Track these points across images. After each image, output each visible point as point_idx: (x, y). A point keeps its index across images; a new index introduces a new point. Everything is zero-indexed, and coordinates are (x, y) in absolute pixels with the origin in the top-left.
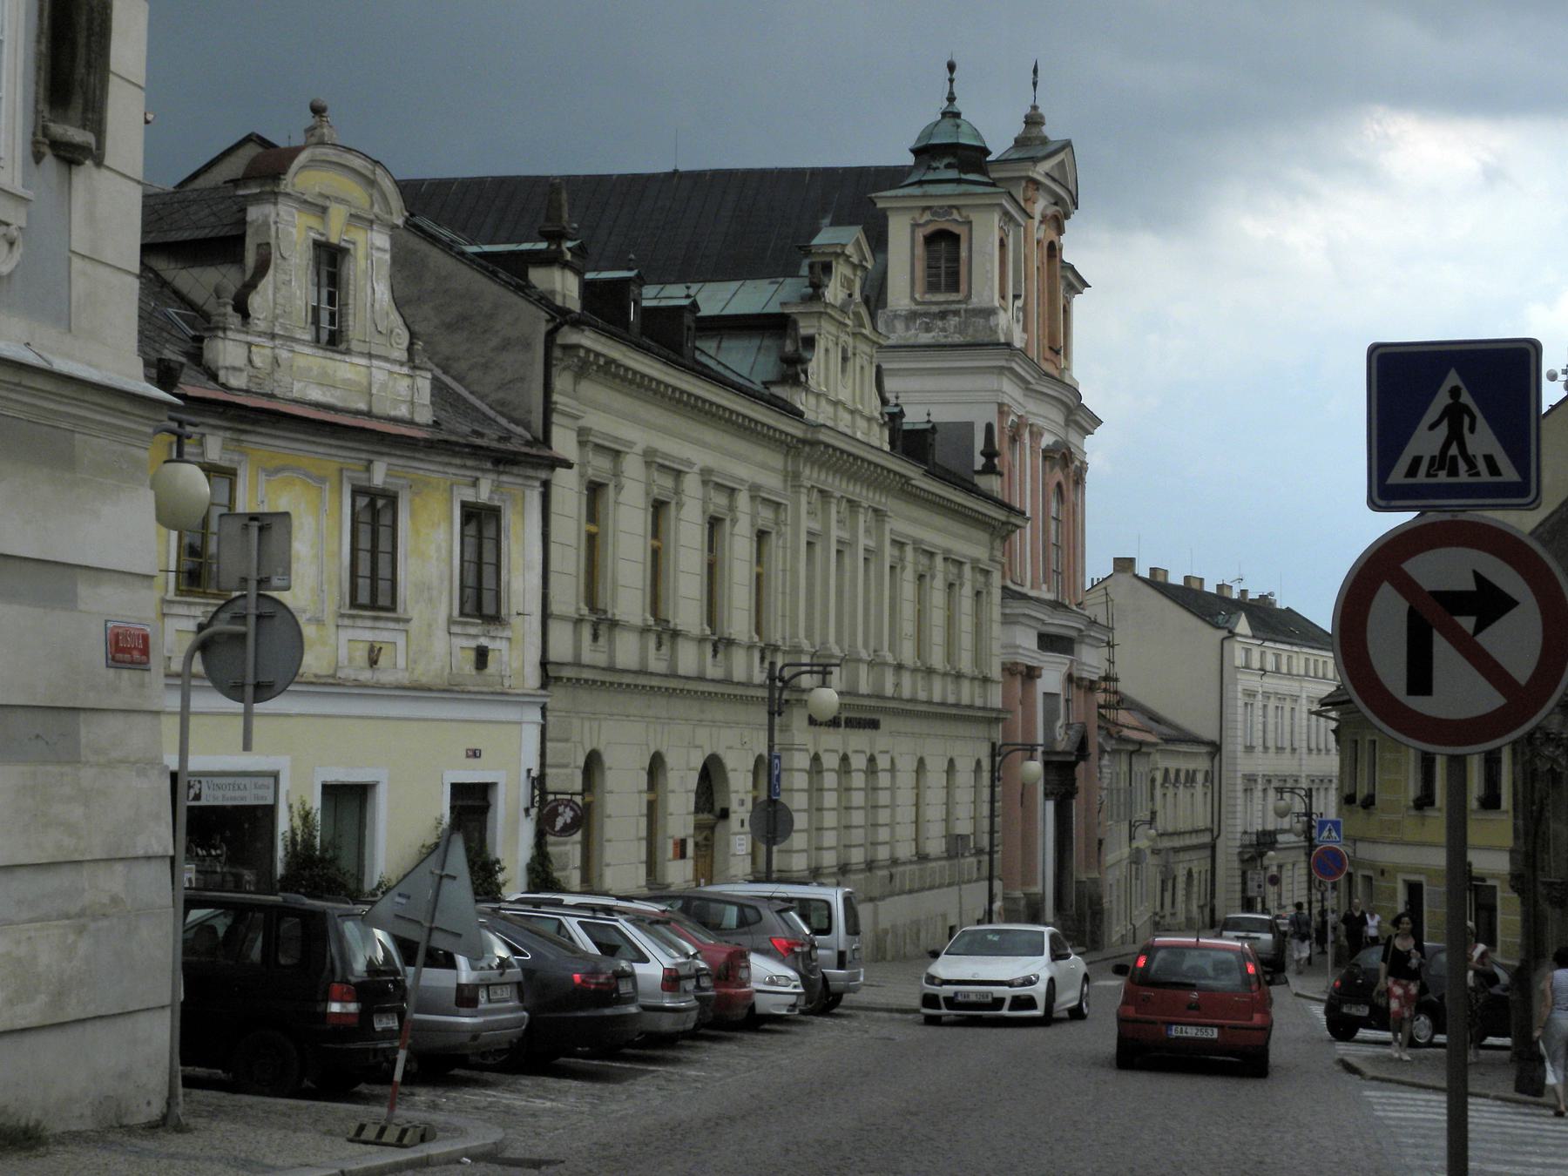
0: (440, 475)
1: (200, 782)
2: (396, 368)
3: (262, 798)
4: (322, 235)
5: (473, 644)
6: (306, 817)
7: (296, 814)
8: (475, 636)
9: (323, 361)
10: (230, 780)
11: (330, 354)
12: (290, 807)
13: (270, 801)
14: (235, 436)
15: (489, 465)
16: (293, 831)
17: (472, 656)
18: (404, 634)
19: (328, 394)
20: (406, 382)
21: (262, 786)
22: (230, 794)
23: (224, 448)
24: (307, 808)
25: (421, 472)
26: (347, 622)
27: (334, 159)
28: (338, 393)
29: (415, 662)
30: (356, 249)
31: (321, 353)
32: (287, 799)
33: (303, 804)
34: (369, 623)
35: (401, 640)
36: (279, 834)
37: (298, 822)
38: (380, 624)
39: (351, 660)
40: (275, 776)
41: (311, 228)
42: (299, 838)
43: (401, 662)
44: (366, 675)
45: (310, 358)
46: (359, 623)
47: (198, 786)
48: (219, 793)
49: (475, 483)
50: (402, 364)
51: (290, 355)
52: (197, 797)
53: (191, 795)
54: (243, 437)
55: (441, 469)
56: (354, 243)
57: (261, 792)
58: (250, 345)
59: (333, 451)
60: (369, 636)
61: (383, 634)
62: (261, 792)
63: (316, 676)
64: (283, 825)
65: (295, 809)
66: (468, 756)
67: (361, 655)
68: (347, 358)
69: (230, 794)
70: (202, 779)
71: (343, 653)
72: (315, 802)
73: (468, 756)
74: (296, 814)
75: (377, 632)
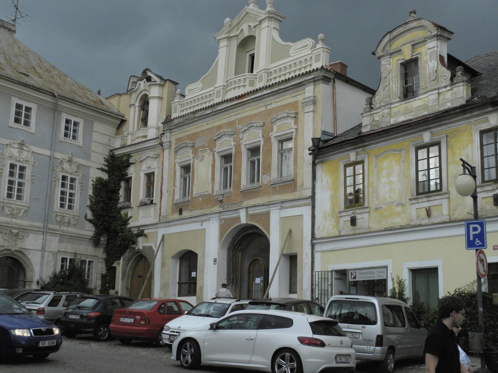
0: (465, 125)
1: (356, 272)
2: (444, 90)
3: (381, 277)
4: (403, 59)
5: (491, 194)
6: (401, 283)
7: (395, 282)
8: (493, 190)
9: (405, 105)
10: (368, 271)
11: (407, 101)
12: (393, 279)
13: (385, 278)
14: (363, 149)
15: (490, 109)
16: (394, 289)
17: (492, 200)
18: (446, 200)
19: (408, 116)
20: (449, 93)
21: (381, 272)
22: (367, 276)
23: (357, 154)
24: (400, 279)
25: (453, 128)
26: (414, 202)
27: (403, 30)
28: (413, 114)
29: (455, 210)
30: (421, 55)
31: (404, 102)
32: (391, 276)
33: (398, 278)
34: (426, 199)
35: (445, 203)
36: (389, 291)
37: (396, 286)
38: (430, 199)
39: (418, 217)
40: (386, 267)
41: (399, 60)
42: (397, 291)
43: (445, 212)
44: (426, 221)
45: (399, 107)
46: (420, 200)
47: (355, 274)
48: (363, 276)
49: (487, 121)
50: (445, 87)
51: (389, 110)
52: (355, 278)
53: (353, 277)
54: (367, 148)
55: (467, 121)
56: (419, 54)
57: (381, 274)
58: (373, 114)
59: (405, 138)
60: (427, 205)
61: (434, 202)
62: (381, 274)
63: (401, 226)
64: (390, 286)
65: (395, 280)
66: (494, 249)
67: (424, 213)
68: (416, 98)
69: (367, 276)
70: (357, 271)
71: (414, 214)
72: (406, 277)
73: (494, 249)
74: (395, 282)
75: (432, 202)
